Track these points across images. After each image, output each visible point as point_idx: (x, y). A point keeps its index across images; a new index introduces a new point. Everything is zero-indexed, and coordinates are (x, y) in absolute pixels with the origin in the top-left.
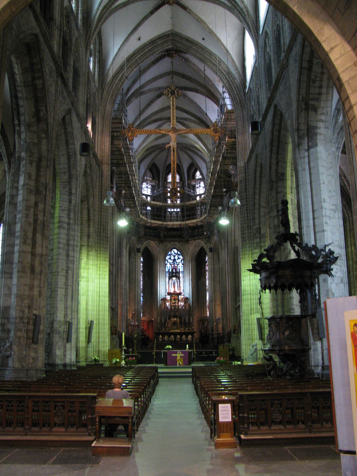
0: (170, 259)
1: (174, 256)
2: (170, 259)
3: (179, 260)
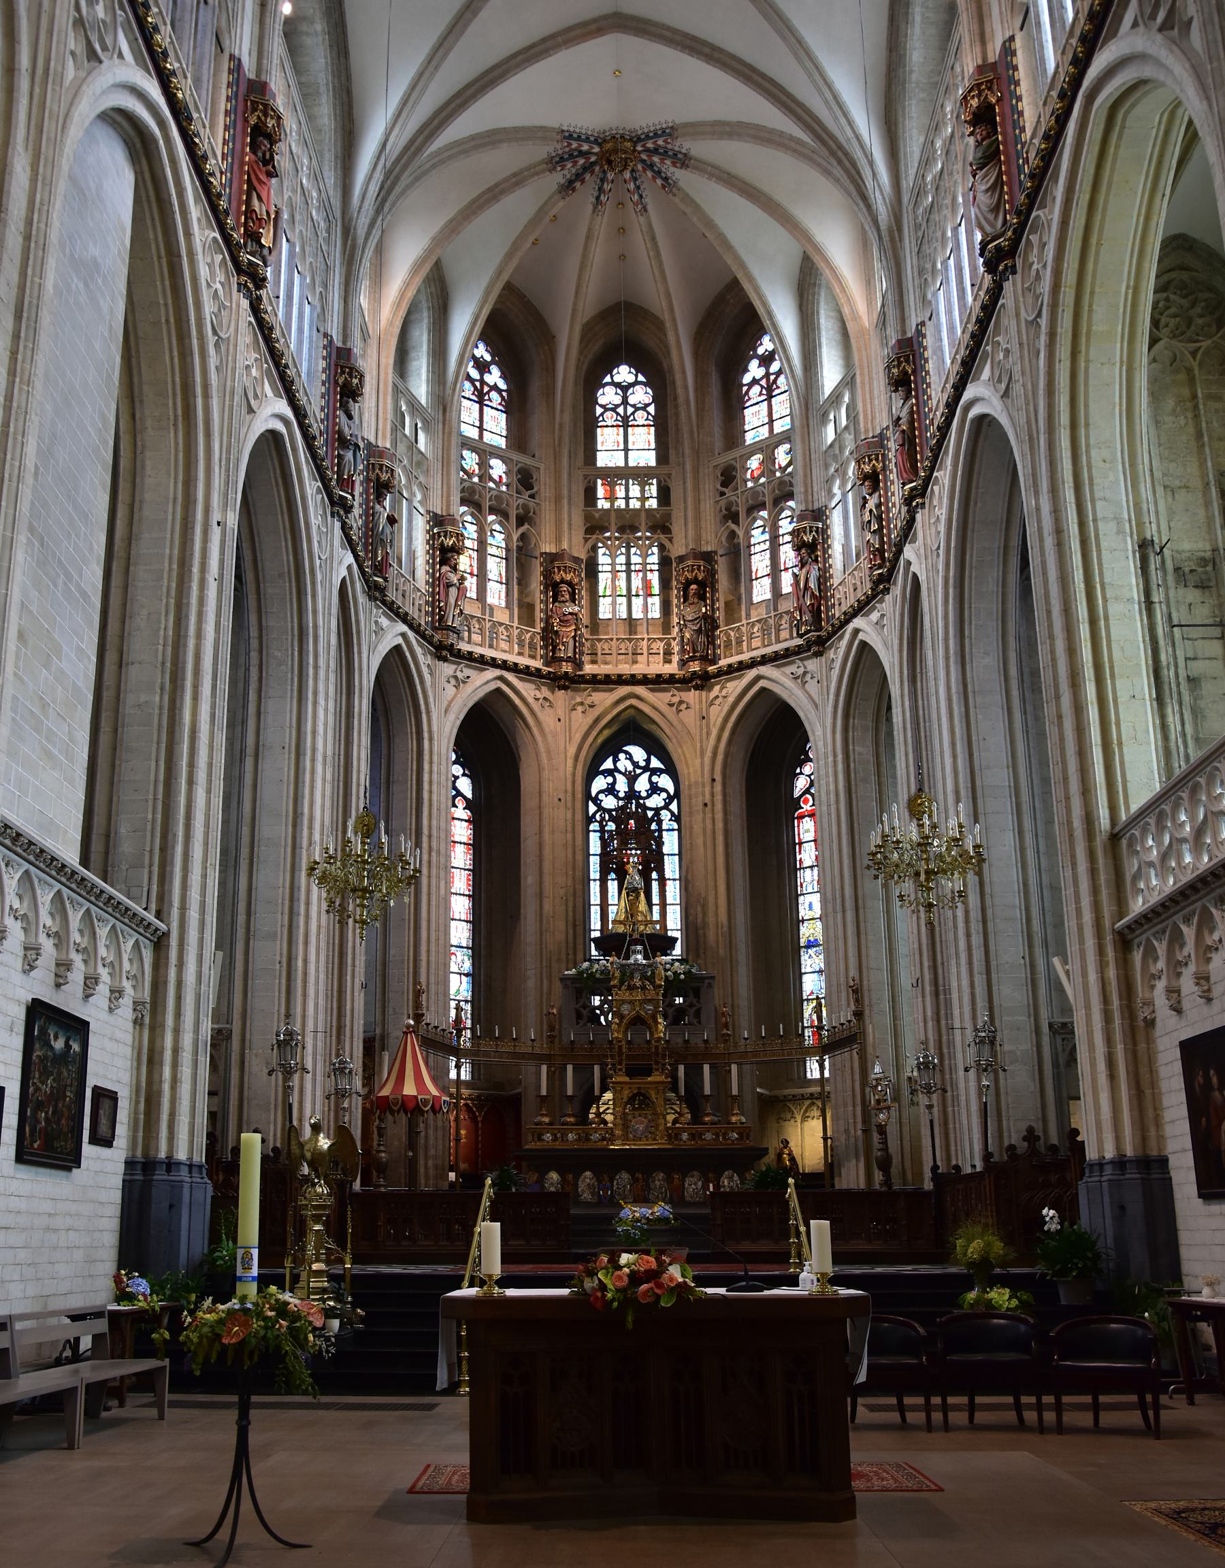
0: (611, 790)
1: (632, 779)
2: (611, 790)
3: (656, 801)
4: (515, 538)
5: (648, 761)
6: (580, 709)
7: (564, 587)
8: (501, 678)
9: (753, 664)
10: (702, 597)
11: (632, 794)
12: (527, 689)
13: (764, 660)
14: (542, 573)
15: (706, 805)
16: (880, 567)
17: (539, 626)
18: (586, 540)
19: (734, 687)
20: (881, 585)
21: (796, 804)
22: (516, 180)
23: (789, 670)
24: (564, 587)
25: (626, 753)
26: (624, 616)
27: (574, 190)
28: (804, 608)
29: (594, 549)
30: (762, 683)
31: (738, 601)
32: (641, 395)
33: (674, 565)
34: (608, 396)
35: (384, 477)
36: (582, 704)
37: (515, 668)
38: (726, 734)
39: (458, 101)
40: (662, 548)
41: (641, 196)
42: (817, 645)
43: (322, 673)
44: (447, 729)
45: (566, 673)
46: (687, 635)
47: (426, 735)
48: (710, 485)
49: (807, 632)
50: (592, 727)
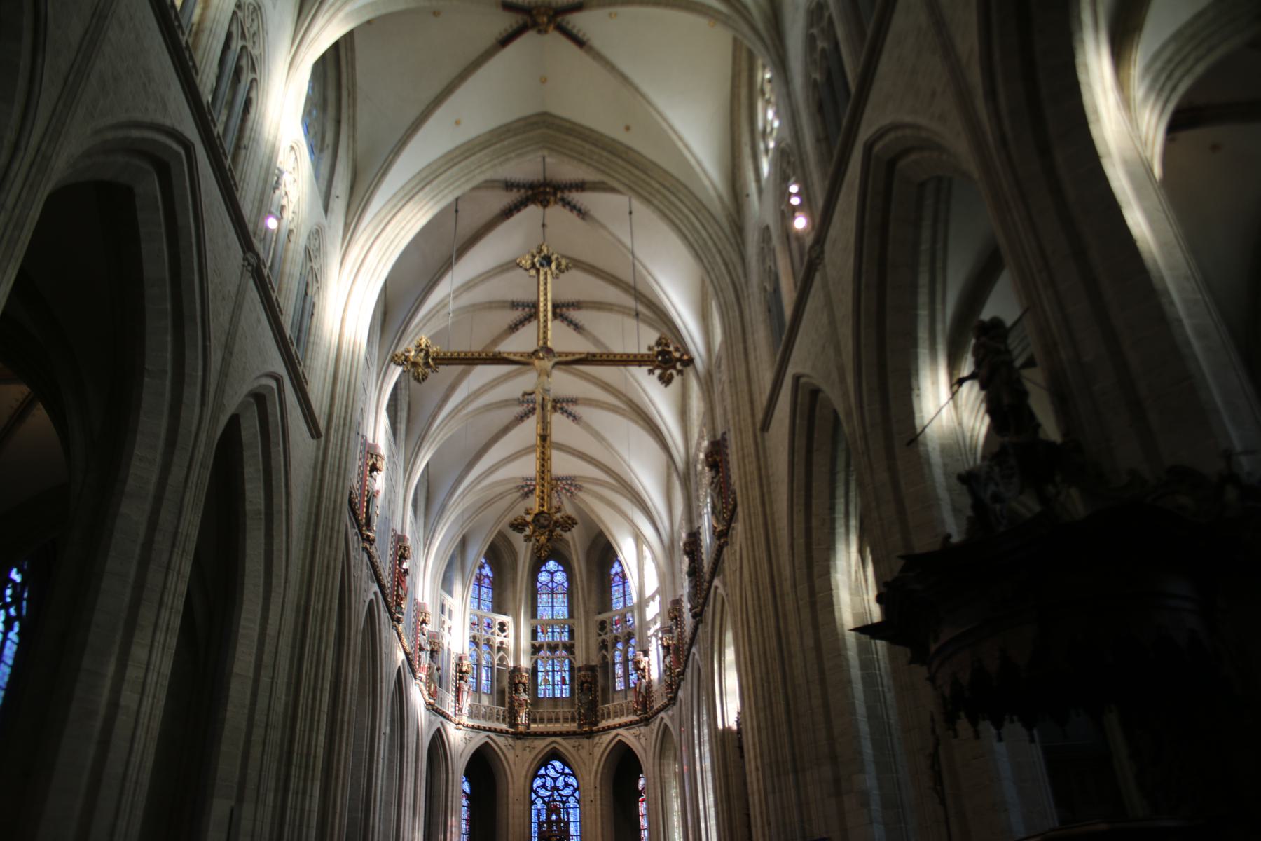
0: (544, 786)
1: (555, 779)
2: (544, 786)
3: (567, 791)
4: (496, 661)
5: (563, 769)
6: (528, 749)
7: (521, 686)
8: (488, 736)
9: (615, 727)
10: (590, 689)
11: (555, 788)
12: (501, 740)
13: (621, 726)
14: (509, 677)
15: (592, 801)
16: (671, 693)
17: (507, 705)
18: (532, 658)
19: (606, 738)
20: (673, 700)
21: (639, 793)
22: (501, 496)
23: (633, 731)
24: (521, 686)
25: (552, 765)
26: (551, 696)
27: (528, 497)
28: (639, 703)
29: (536, 662)
30: (619, 738)
31: (608, 690)
32: (560, 577)
33: (576, 672)
34: (543, 577)
35: (436, 648)
36: (529, 747)
37: (495, 731)
38: (602, 763)
39: (477, 481)
40: (570, 662)
41: (560, 498)
42: (646, 721)
43: (409, 764)
44: (461, 767)
45: (521, 732)
46: (582, 711)
47: (450, 771)
48: (594, 630)
49: (640, 714)
50: (534, 759)
